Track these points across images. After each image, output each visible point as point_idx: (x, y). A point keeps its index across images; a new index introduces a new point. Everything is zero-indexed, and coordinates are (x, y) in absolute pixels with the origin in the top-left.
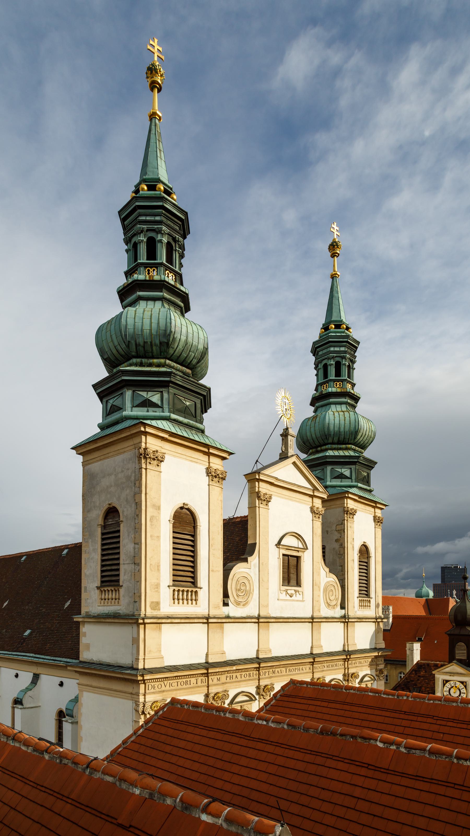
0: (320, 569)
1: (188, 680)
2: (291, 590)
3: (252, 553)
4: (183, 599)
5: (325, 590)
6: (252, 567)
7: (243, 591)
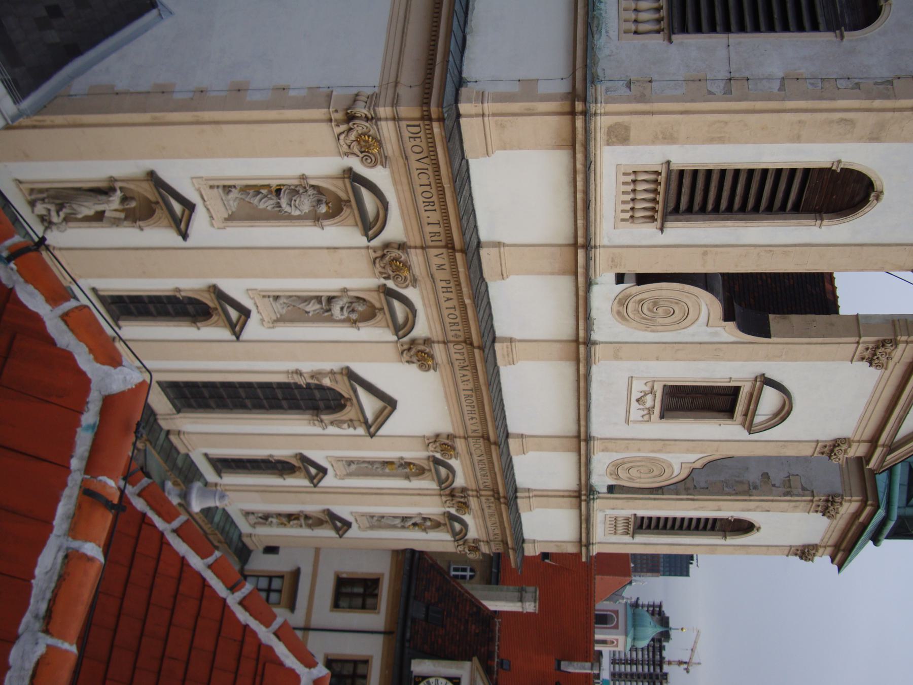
0: (702, 452)
1: (436, 207)
2: (655, 402)
6: (709, 330)
7: (655, 313)
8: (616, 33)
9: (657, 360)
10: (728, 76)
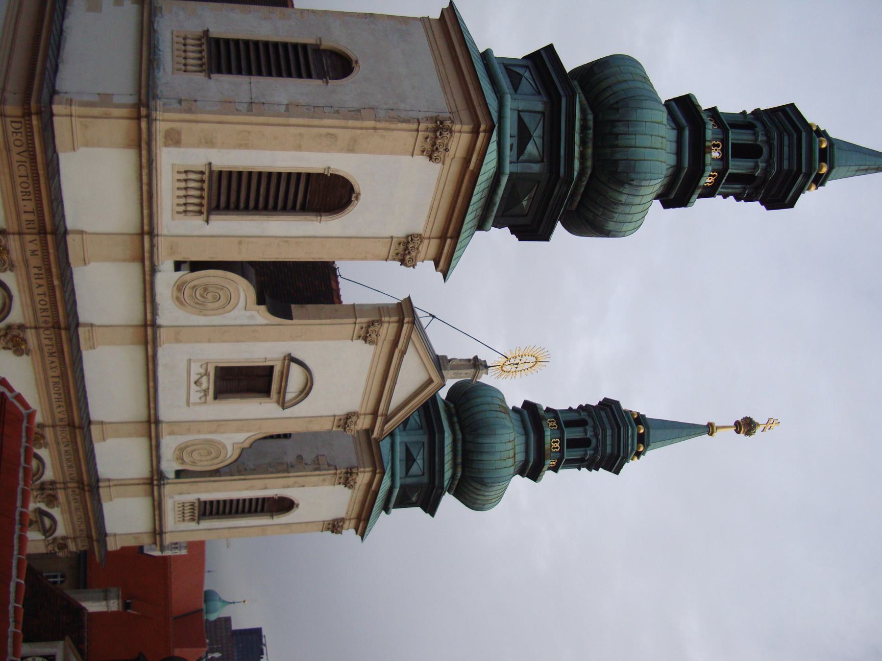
0: (248, 431)
1: (32, 197)
2: (209, 383)
4: (186, 189)
5: (211, 442)
6: (248, 313)
7: (204, 297)
8: (171, 70)
9: (209, 341)
10: (251, 101)
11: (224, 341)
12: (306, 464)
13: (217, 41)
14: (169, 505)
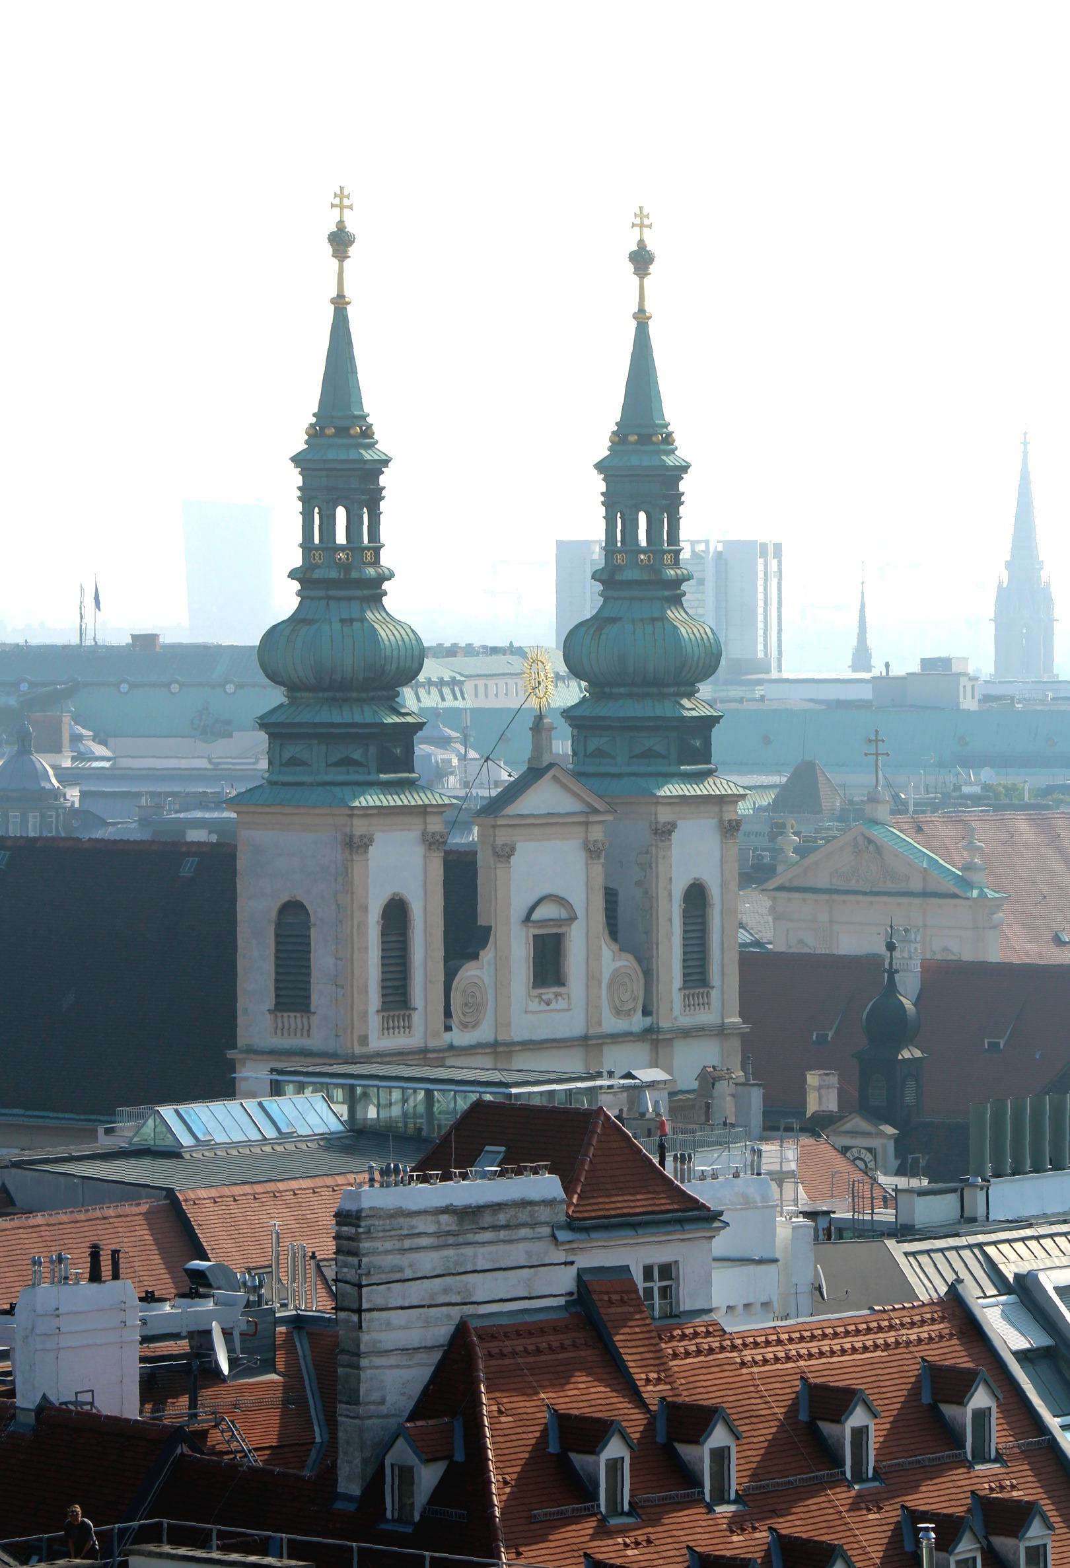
2: (549, 993)
3: (484, 943)
5: (611, 985)
6: (486, 966)
9: (509, 997)
11: (510, 984)
12: (645, 877)
13: (277, 1004)
14: (686, 1021)
